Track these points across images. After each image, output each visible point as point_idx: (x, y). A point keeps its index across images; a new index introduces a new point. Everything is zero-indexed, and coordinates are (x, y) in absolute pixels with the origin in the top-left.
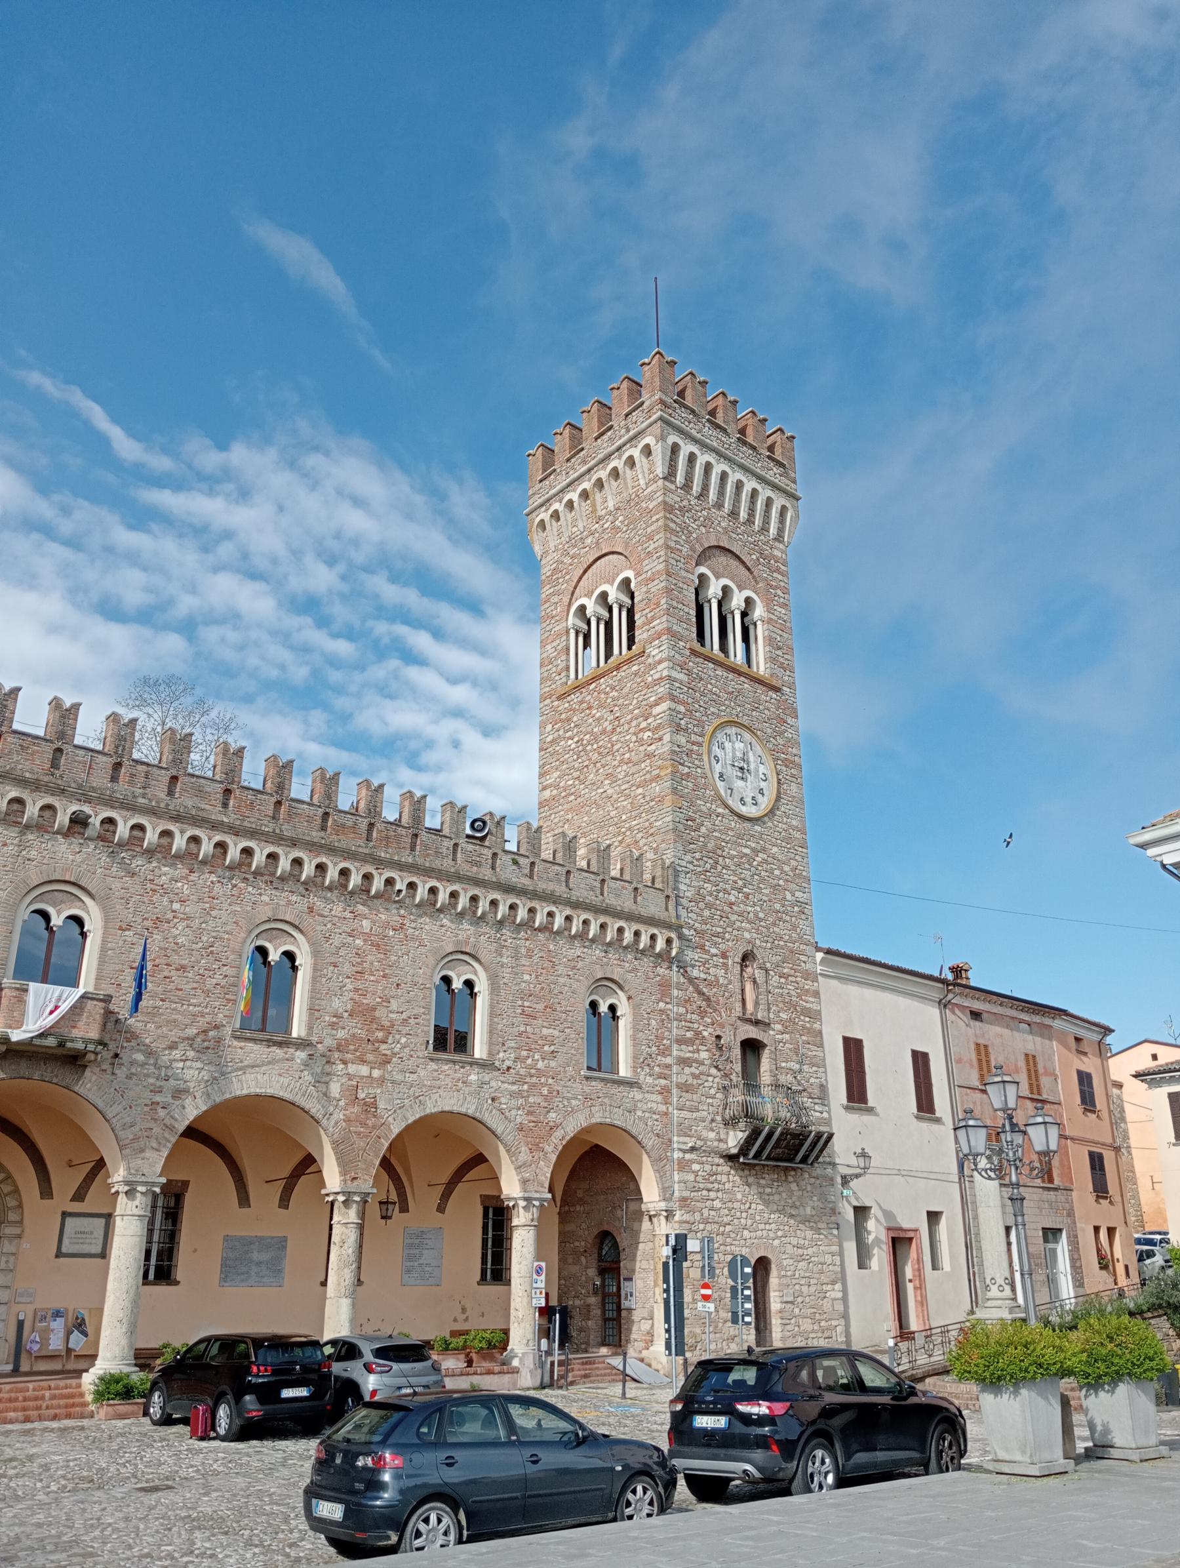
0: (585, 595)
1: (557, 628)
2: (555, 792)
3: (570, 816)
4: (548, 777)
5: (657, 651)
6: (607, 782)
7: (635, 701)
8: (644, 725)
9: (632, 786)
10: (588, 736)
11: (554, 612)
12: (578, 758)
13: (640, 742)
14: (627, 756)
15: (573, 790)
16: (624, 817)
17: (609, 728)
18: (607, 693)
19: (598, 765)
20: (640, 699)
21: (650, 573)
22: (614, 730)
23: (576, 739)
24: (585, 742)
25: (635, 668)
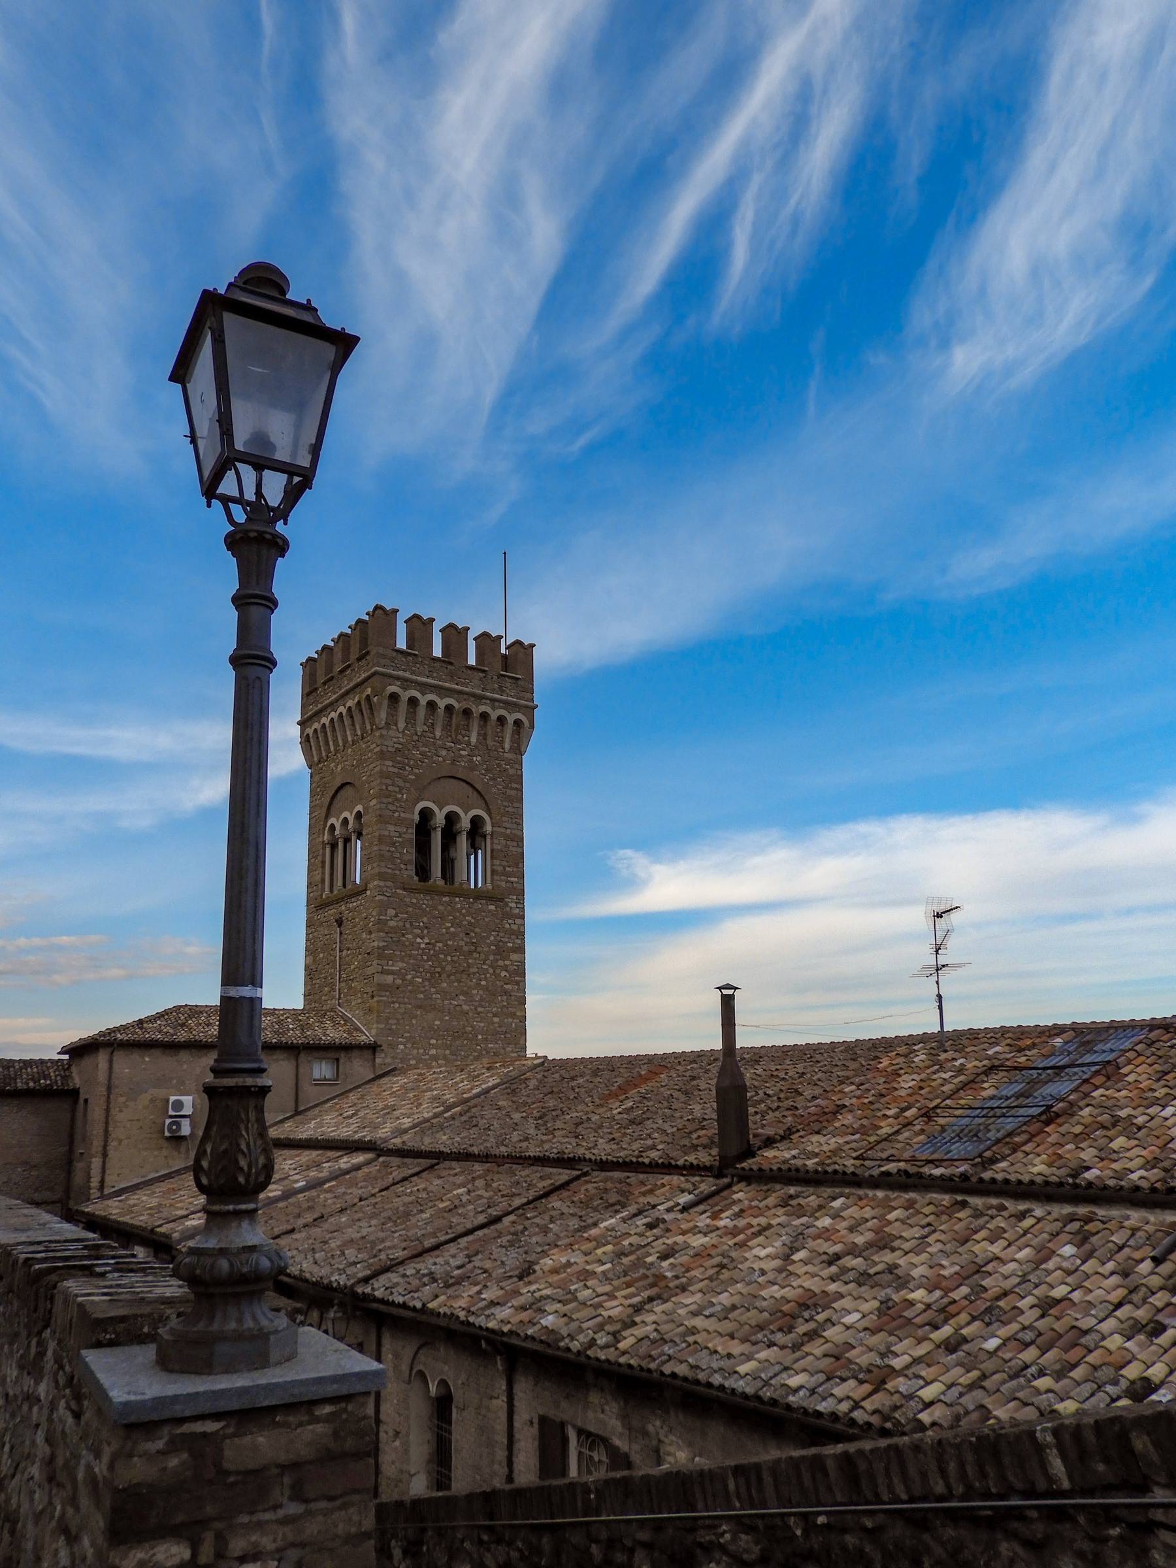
0: (434, 802)
1: (403, 815)
2: (399, 982)
3: (419, 1013)
4: (390, 963)
5: (513, 905)
6: (462, 997)
7: (492, 938)
8: (501, 963)
9: (488, 1012)
10: (441, 945)
11: (399, 796)
12: (428, 961)
13: (497, 976)
14: (483, 983)
15: (423, 989)
16: (480, 1037)
17: (466, 948)
18: (464, 916)
19: (453, 977)
20: (498, 938)
21: (508, 831)
22: (470, 953)
23: (427, 941)
24: (437, 948)
25: (492, 907)
